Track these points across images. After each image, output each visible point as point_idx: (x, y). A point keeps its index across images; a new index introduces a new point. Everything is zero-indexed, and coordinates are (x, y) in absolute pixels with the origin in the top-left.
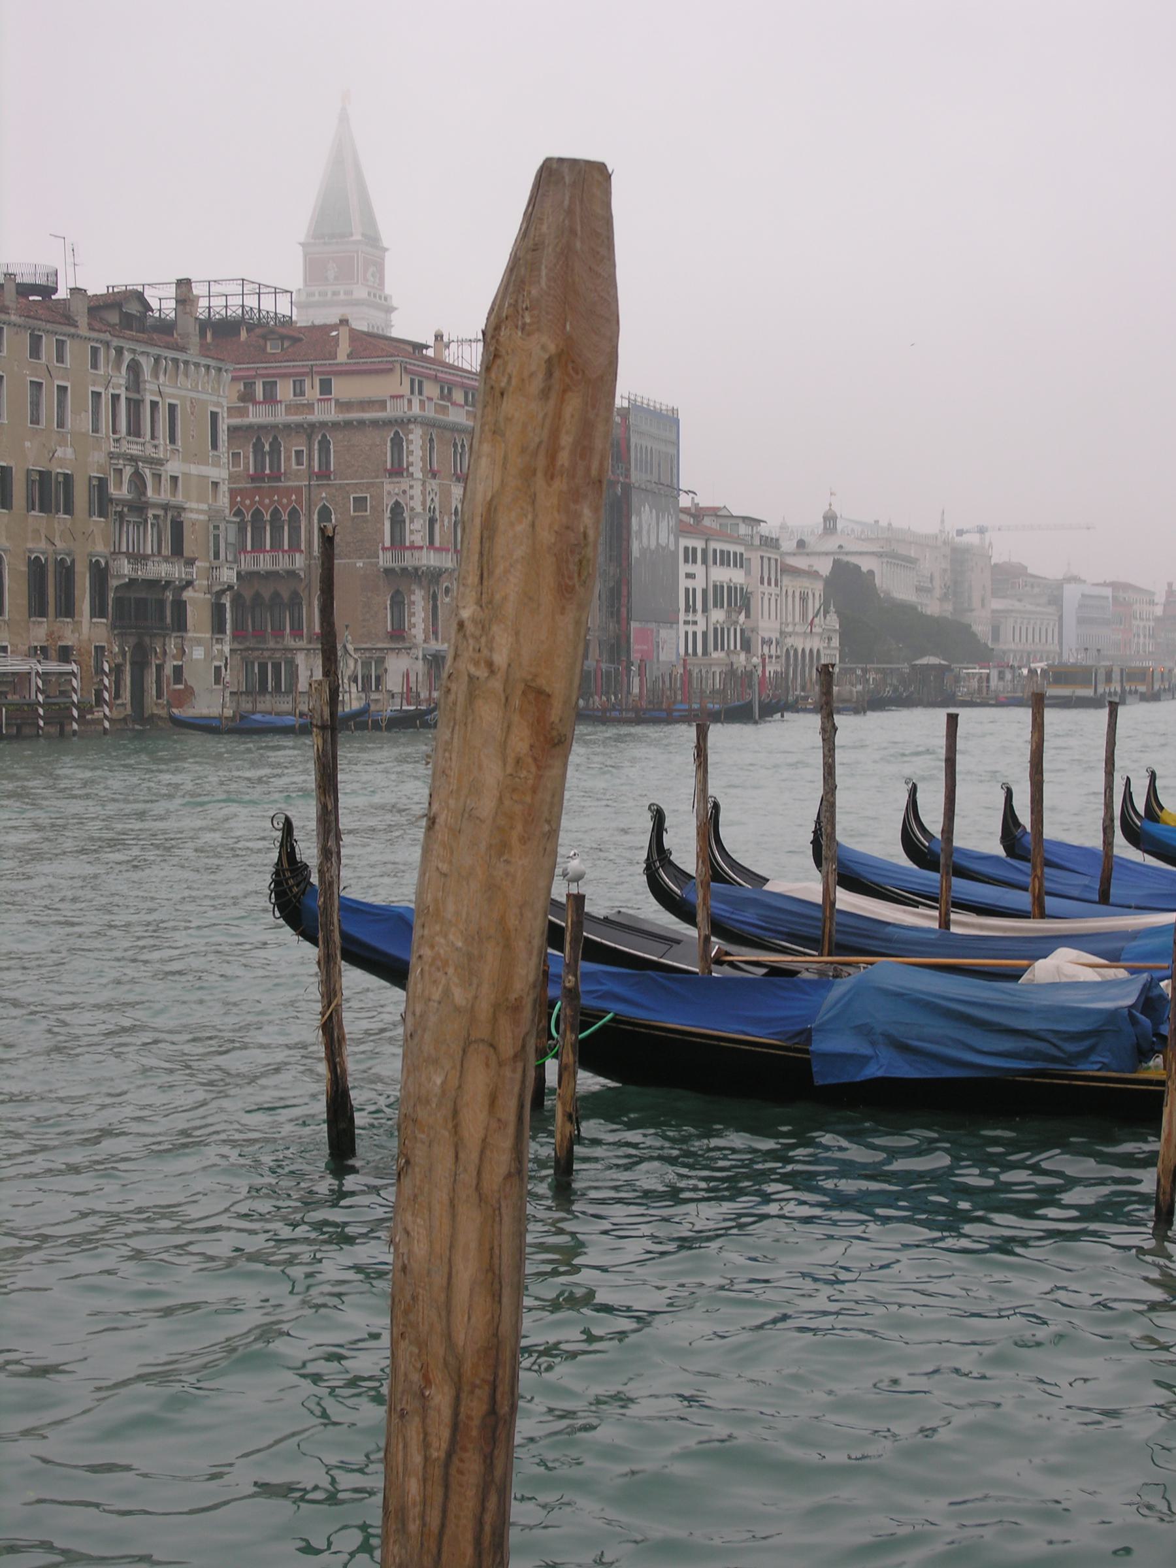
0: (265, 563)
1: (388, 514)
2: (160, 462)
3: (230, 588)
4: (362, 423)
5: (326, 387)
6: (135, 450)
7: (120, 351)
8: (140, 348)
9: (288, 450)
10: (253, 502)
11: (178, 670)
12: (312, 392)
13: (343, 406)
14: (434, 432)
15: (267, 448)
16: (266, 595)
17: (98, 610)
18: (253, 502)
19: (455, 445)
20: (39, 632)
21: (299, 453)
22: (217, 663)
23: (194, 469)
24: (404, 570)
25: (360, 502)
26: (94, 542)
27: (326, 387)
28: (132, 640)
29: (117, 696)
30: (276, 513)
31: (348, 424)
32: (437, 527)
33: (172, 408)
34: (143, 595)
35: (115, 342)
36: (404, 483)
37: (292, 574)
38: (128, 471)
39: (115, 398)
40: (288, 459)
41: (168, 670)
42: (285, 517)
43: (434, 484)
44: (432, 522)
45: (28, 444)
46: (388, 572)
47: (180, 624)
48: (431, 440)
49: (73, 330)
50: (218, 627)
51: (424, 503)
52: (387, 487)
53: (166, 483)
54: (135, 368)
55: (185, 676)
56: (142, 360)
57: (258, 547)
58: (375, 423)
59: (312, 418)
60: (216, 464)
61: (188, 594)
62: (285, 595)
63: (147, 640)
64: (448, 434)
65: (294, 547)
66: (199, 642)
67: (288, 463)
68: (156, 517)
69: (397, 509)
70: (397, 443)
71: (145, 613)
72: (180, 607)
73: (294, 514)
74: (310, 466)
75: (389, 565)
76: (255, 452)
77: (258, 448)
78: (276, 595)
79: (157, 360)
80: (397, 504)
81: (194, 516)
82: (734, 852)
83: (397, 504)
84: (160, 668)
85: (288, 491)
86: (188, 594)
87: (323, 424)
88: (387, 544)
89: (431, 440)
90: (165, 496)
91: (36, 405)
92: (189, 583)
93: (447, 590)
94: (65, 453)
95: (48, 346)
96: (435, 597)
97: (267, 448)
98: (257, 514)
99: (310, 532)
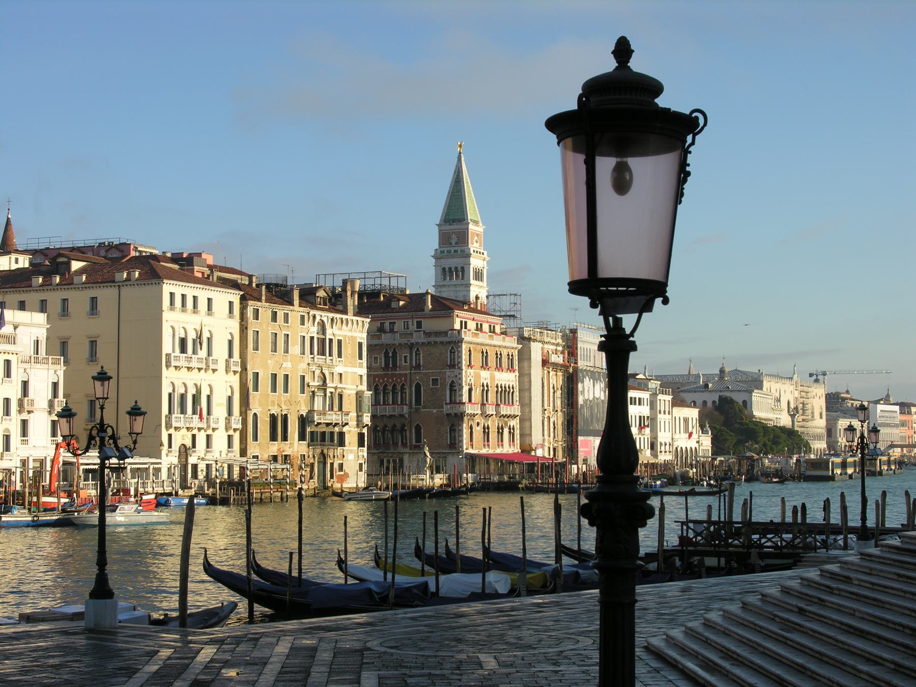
3: (367, 425)
6: (321, 362)
7: (314, 317)
8: (324, 314)
11: (341, 467)
17: (302, 437)
23: (350, 370)
28: (319, 451)
33: (340, 342)
34: (324, 430)
35: (312, 312)
38: (318, 372)
39: (312, 338)
41: (336, 466)
47: (342, 443)
50: (361, 444)
53: (336, 377)
54: (322, 325)
56: (325, 319)
60: (361, 366)
61: (345, 429)
66: (351, 451)
68: (331, 393)
71: (325, 439)
72: (342, 435)
79: (332, 320)
84: (332, 464)
86: (345, 429)
90: (336, 383)
92: (347, 424)
94: (287, 365)
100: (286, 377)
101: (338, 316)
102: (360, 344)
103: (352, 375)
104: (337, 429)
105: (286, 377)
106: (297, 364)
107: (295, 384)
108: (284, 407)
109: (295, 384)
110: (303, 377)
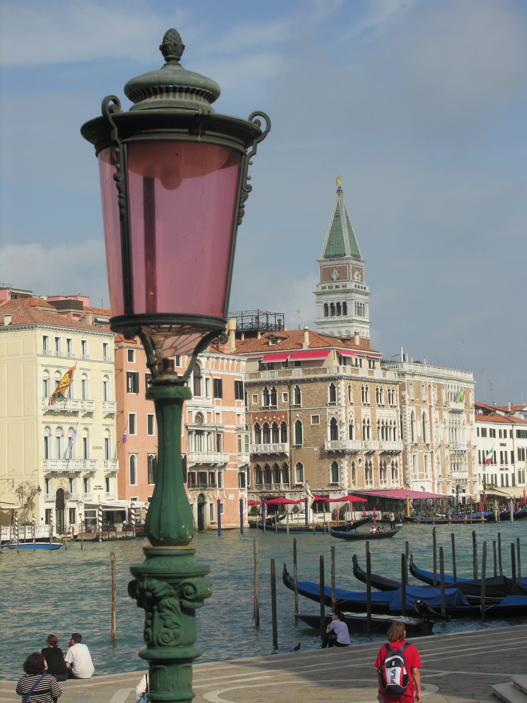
9: (280, 394)
14: (352, 383)
15: (270, 393)
21: (285, 395)
24: (337, 451)
25: (316, 418)
30: (275, 425)
31: (309, 381)
32: (354, 429)
36: (336, 409)
37: (283, 455)
40: (280, 398)
42: (279, 426)
43: (351, 408)
44: (351, 427)
48: (349, 387)
51: (346, 418)
58: (322, 380)
59: (291, 378)
60: (239, 405)
64: (360, 382)
65: (284, 440)
67: (281, 400)
69: (334, 421)
70: (333, 388)
73: (284, 425)
75: (332, 449)
76: (264, 395)
77: (266, 391)
80: (333, 419)
83: (333, 419)
85: (281, 413)
87: (297, 381)
89: (349, 387)
93: (360, 460)
96: (353, 465)
97: (270, 393)
98: (266, 426)
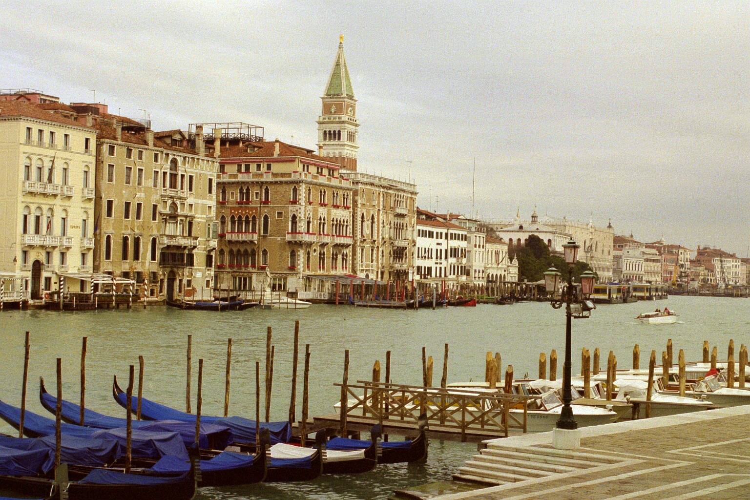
0: (242, 237)
1: (290, 219)
2: (184, 199)
3: (214, 249)
4: (281, 182)
5: (269, 167)
6: (173, 194)
7: (167, 155)
9: (252, 192)
10: (238, 213)
11: (189, 282)
12: (264, 168)
13: (275, 175)
15: (245, 191)
16: (242, 250)
18: (238, 213)
19: (321, 192)
20: (126, 267)
21: (257, 193)
22: (208, 279)
23: (200, 201)
24: (296, 242)
25: (280, 214)
26: (152, 230)
27: (269, 167)
28: (168, 270)
29: (161, 291)
30: (247, 217)
31: (276, 182)
32: (311, 225)
33: (191, 177)
34: (174, 251)
35: (165, 151)
36: (297, 206)
37: (252, 242)
38: (169, 202)
39: (165, 173)
40: (253, 196)
41: (185, 282)
42: (251, 219)
43: (310, 207)
44: (309, 223)
45: (124, 192)
46: (290, 242)
47: (191, 263)
48: (309, 190)
49: (146, 147)
50: (209, 262)
51: (305, 215)
52: (290, 208)
53: (187, 207)
54: (174, 162)
55: (192, 284)
56: (178, 158)
57: (240, 232)
58: (287, 183)
59: (262, 180)
60: (211, 199)
61: (194, 252)
62: (249, 251)
63: (175, 270)
65: (254, 231)
66: (199, 270)
67: (253, 197)
68: (181, 220)
69: (294, 217)
70: (295, 190)
71: (175, 258)
72: (191, 257)
73: (254, 218)
74: (261, 199)
75: (290, 240)
76: (240, 192)
77: (241, 190)
78: (246, 251)
79: (185, 158)
80: (294, 215)
81: (199, 220)
82: (113, 403)
83: (294, 215)
84: (181, 281)
85: (252, 208)
86: (194, 252)
87: (267, 182)
88: (290, 231)
89: (309, 190)
90: (186, 212)
91: (128, 176)
92: (195, 247)
93: (315, 250)
94: (141, 196)
95: (135, 153)
96: (309, 253)
97: (245, 191)
98: (240, 217)
99: (260, 225)
100: (139, 205)
101: (191, 156)
102: (210, 180)
103: (202, 206)
104: (186, 252)
105: (139, 205)
106: (149, 193)
107: (146, 212)
108: (137, 231)
109: (146, 212)
110: (155, 207)
